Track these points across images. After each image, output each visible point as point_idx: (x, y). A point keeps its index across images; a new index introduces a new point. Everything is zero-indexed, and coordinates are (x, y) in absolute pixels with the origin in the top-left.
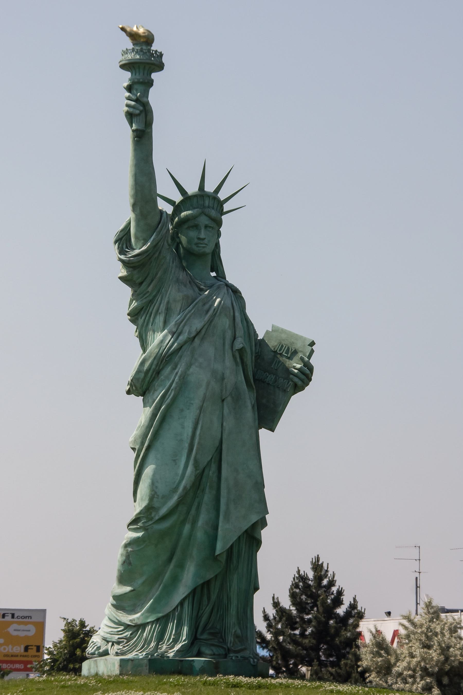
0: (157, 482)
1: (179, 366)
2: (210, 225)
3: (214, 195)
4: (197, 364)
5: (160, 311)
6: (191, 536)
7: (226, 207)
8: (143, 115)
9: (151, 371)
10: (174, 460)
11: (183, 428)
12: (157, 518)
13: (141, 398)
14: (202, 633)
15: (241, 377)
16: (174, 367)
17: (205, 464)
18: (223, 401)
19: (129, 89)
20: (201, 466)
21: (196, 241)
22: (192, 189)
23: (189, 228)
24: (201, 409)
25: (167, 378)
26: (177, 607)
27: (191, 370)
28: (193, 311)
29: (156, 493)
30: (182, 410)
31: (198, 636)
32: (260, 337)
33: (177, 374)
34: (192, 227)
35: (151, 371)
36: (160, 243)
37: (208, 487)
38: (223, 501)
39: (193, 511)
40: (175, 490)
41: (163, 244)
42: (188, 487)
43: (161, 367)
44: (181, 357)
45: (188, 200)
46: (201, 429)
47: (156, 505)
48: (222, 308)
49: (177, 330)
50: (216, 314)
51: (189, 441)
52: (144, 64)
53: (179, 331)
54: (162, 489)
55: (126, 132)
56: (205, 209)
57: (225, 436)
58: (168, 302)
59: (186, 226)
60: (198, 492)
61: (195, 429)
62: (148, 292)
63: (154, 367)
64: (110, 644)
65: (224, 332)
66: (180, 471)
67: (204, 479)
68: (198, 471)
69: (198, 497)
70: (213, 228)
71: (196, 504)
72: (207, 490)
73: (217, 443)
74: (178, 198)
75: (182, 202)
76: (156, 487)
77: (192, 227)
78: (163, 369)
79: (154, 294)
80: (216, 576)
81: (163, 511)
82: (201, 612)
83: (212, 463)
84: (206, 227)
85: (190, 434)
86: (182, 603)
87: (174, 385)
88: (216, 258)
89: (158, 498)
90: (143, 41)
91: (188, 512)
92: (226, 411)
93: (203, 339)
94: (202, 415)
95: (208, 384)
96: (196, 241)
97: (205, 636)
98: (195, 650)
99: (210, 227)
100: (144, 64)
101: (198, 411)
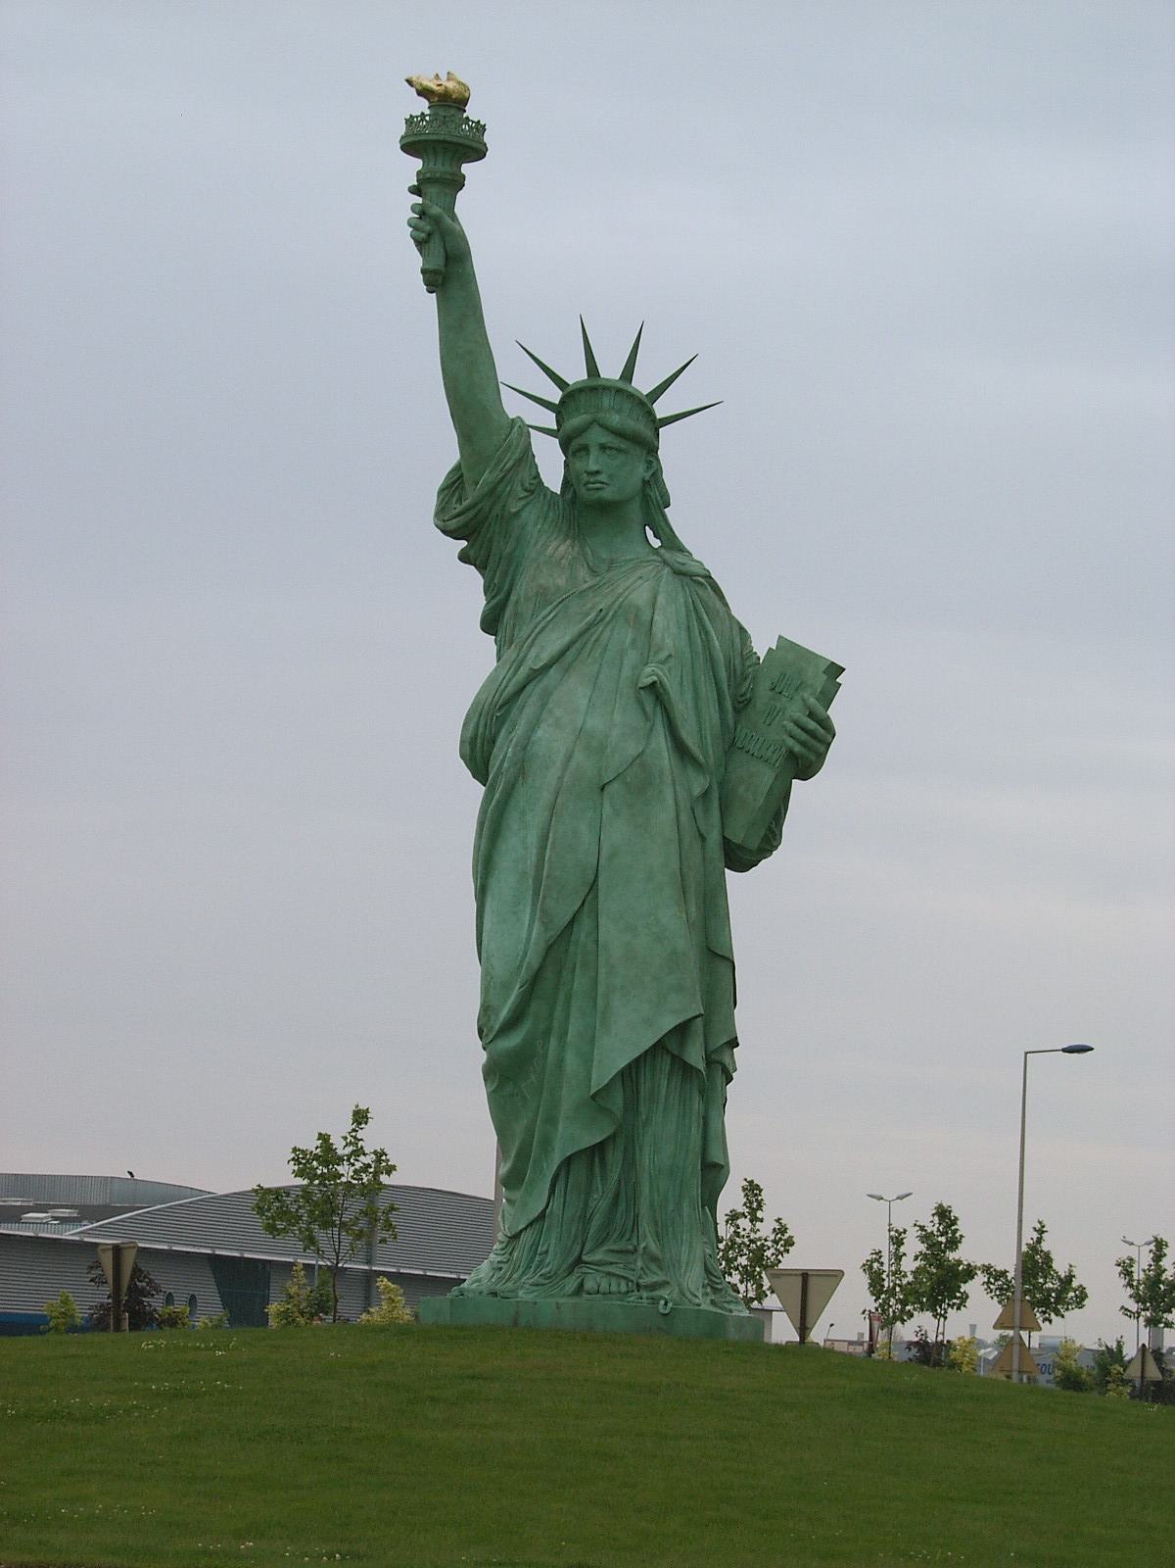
2: (610, 445)
3: (621, 385)
4: (551, 721)
7: (661, 409)
10: (515, 913)
12: (497, 1027)
14: (591, 1251)
15: (661, 742)
18: (603, 789)
22: (575, 373)
24: (553, 807)
27: (540, 733)
30: (523, 813)
31: (585, 1258)
33: (511, 741)
34: (578, 450)
35: (479, 740)
38: (601, 989)
39: (558, 1013)
48: (620, 607)
52: (445, 140)
61: (543, 848)
63: (481, 730)
66: (524, 934)
67: (572, 949)
68: (552, 933)
70: (619, 450)
71: (561, 998)
74: (555, 395)
75: (563, 401)
77: (578, 450)
78: (498, 732)
80: (613, 1137)
81: (504, 1013)
84: (603, 447)
87: (506, 765)
88: (653, 511)
92: (607, 809)
95: (569, 758)
97: (598, 1256)
98: (571, 1284)
99: (611, 448)
100: (445, 140)
101: (546, 813)
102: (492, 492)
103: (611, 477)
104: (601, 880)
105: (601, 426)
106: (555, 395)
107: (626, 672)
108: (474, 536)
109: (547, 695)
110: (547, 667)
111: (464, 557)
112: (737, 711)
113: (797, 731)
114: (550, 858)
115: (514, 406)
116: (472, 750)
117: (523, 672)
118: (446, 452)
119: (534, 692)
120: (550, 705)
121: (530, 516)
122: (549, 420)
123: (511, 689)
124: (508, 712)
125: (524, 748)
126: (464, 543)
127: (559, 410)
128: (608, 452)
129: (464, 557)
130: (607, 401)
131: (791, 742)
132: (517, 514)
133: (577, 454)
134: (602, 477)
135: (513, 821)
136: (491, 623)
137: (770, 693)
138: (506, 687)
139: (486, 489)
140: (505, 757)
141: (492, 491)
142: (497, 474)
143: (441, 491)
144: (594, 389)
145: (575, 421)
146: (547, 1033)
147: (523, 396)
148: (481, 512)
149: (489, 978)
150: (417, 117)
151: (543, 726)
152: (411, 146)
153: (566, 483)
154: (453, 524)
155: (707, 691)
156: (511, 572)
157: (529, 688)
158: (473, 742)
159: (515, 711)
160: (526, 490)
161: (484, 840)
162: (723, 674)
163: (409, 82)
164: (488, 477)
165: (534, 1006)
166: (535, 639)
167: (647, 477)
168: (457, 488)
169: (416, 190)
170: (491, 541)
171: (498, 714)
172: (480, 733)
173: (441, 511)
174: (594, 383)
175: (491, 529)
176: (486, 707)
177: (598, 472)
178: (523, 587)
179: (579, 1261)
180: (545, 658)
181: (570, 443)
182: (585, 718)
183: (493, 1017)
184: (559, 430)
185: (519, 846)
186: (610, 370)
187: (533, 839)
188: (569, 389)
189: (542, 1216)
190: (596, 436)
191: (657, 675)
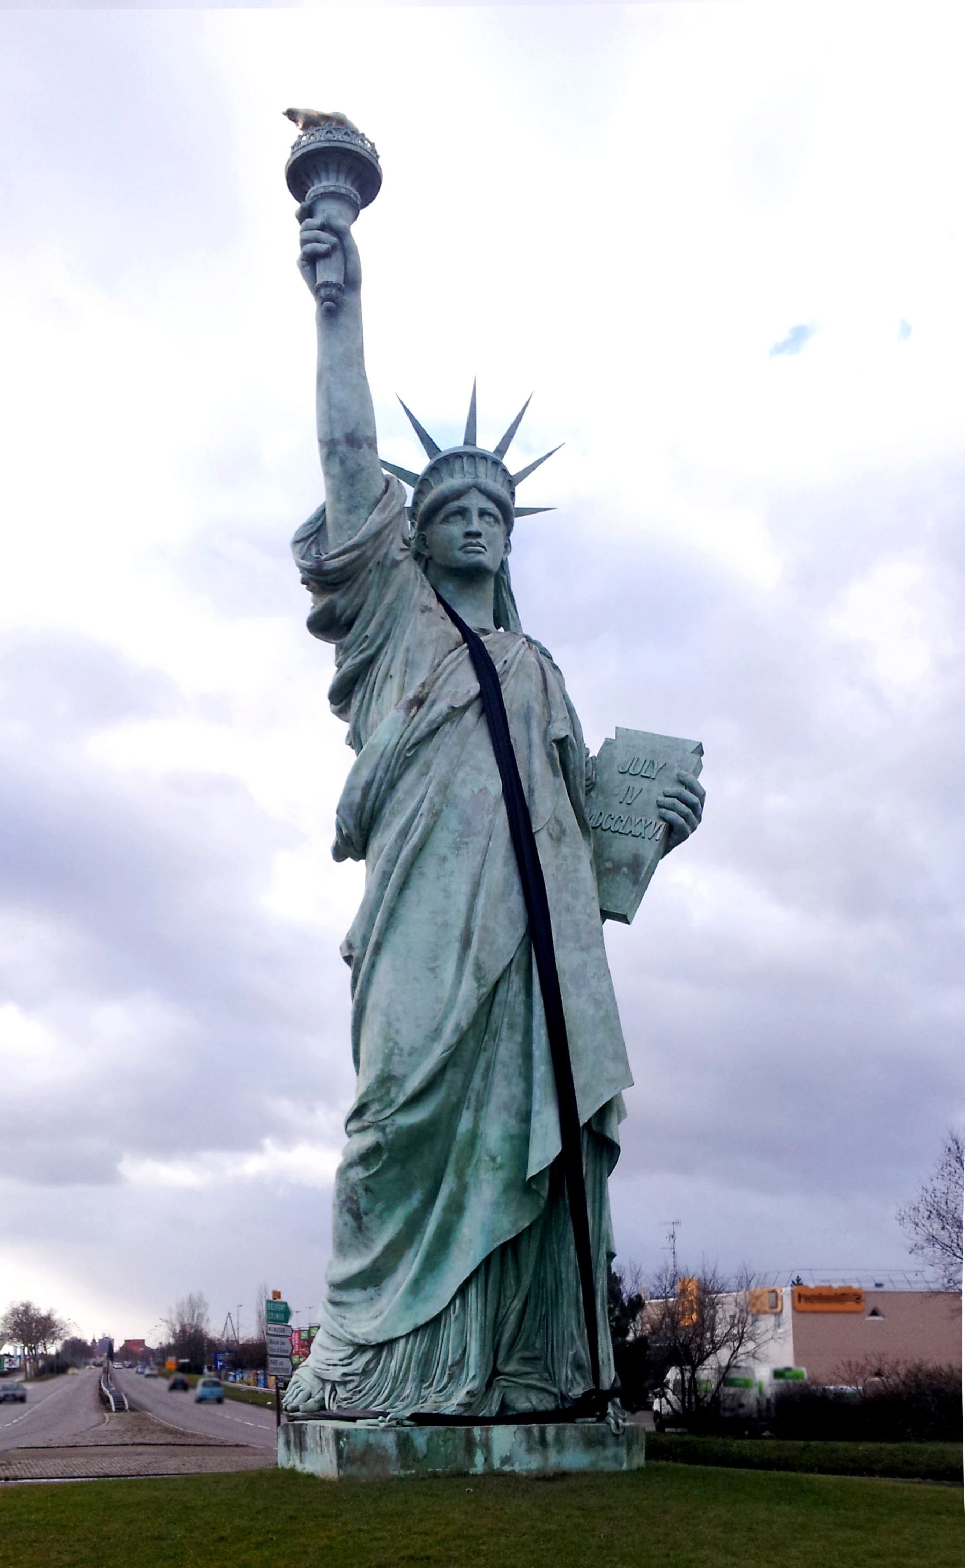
0: (398, 1019)
1: (434, 767)
4: (471, 763)
5: (392, 672)
6: (474, 1137)
10: (433, 970)
11: (448, 896)
13: (362, 862)
17: (500, 970)
20: (492, 978)
23: (446, 520)
25: (409, 793)
26: (453, 1301)
29: (396, 1043)
30: (444, 859)
35: (375, 785)
37: (505, 1026)
39: (477, 1082)
40: (436, 1033)
42: (464, 1024)
43: (396, 773)
47: (398, 1071)
51: (460, 923)
54: (409, 1035)
55: (305, 305)
58: (408, 650)
59: (441, 515)
60: (486, 1038)
61: (474, 895)
62: (367, 637)
63: (380, 773)
64: (328, 1387)
66: (446, 992)
67: (496, 1010)
68: (484, 990)
69: (485, 1050)
71: (481, 1064)
72: (504, 1033)
76: (397, 1032)
78: (400, 777)
82: (502, 1312)
83: (513, 973)
84: (483, 513)
86: (462, 1291)
89: (401, 1055)
91: (465, 1087)
96: (462, 541)
99: (490, 514)
101: (479, 858)
102: (376, 535)
103: (489, 543)
108: (349, 583)
117: (441, 707)
124: (416, 754)
125: (447, 787)
128: (487, 518)
130: (482, 467)
133: (451, 519)
134: (482, 541)
135: (430, 866)
146: (454, 1111)
147: (401, 451)
149: (391, 1044)
156: (387, 626)
165: (449, 1076)
170: (369, 589)
172: (377, 778)
174: (469, 449)
175: (371, 578)
176: (388, 748)
177: (479, 535)
179: (495, 1373)
183: (394, 1091)
188: (440, 456)
189: (435, 1323)
190: (475, 502)
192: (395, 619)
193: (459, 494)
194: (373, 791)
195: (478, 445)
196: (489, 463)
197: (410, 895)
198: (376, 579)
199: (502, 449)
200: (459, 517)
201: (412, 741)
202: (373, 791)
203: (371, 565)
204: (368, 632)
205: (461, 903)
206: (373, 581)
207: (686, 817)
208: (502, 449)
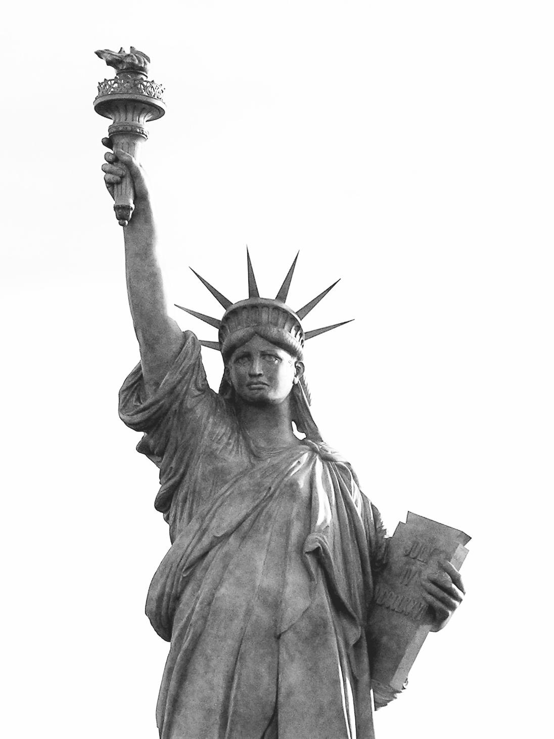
4: (231, 580)
8: (127, 181)
9: (165, 598)
15: (323, 598)
16: (196, 587)
18: (278, 637)
19: (108, 143)
21: (248, 379)
22: (238, 294)
24: (238, 656)
27: (223, 590)
28: (228, 493)
32: (390, 534)
33: (198, 598)
34: (242, 357)
35: (165, 598)
36: (179, 388)
41: (187, 389)
43: (179, 589)
44: (206, 569)
45: (234, 312)
46: (238, 687)
49: (200, 527)
50: (272, 496)
53: (204, 527)
56: (256, 327)
57: (281, 699)
61: (229, 688)
62: (172, 467)
63: (167, 589)
65: (288, 524)
73: (270, 713)
74: (219, 313)
75: (226, 318)
77: (242, 357)
79: (181, 471)
85: (221, 698)
87: (194, 618)
88: (300, 407)
90: (129, 66)
92: (284, 656)
93: (243, 538)
94: (238, 663)
95: (248, 612)
104: (281, 716)
105: (262, 337)
106: (219, 313)
107: (294, 539)
109: (228, 556)
110: (227, 536)
111: (143, 448)
112: (375, 575)
113: (434, 588)
114: (236, 697)
115: (183, 322)
116: (159, 606)
118: (128, 356)
119: (216, 556)
120: (231, 567)
121: (201, 411)
122: (212, 334)
123: (197, 553)
124: (192, 574)
125: (209, 604)
126: (141, 434)
127: (222, 326)
129: (143, 448)
131: (430, 598)
132: (192, 410)
135: (199, 665)
136: (163, 504)
137: (404, 559)
138: (189, 555)
139: (167, 388)
140: (193, 610)
141: (172, 390)
142: (178, 376)
143: (121, 392)
144: (254, 307)
145: (238, 333)
148: (157, 409)
150: (111, 80)
151: (226, 584)
152: (103, 108)
153: (225, 384)
154: (138, 418)
155: (353, 557)
157: (211, 553)
158: (160, 599)
159: (198, 574)
160: (199, 390)
161: (173, 683)
162: (365, 543)
163: (99, 54)
164: (169, 379)
166: (216, 511)
167: (297, 380)
168: (136, 389)
169: (108, 143)
170: (168, 431)
171: (184, 575)
173: (124, 407)
175: (170, 423)
177: (260, 375)
178: (199, 469)
180: (225, 527)
181: (231, 353)
182: (261, 578)
184: (220, 343)
185: (208, 684)
186: (268, 291)
187: (219, 680)
191: (320, 542)
192: (191, 453)
193: (243, 342)
194: (164, 603)
195: (261, 296)
196: (271, 310)
197: (188, 687)
198: (175, 422)
199: (283, 294)
200: (246, 359)
201: (187, 565)
202: (164, 603)
203: (169, 413)
204: (173, 465)
205: (220, 692)
206: (172, 424)
207: (442, 600)
208: (283, 294)
